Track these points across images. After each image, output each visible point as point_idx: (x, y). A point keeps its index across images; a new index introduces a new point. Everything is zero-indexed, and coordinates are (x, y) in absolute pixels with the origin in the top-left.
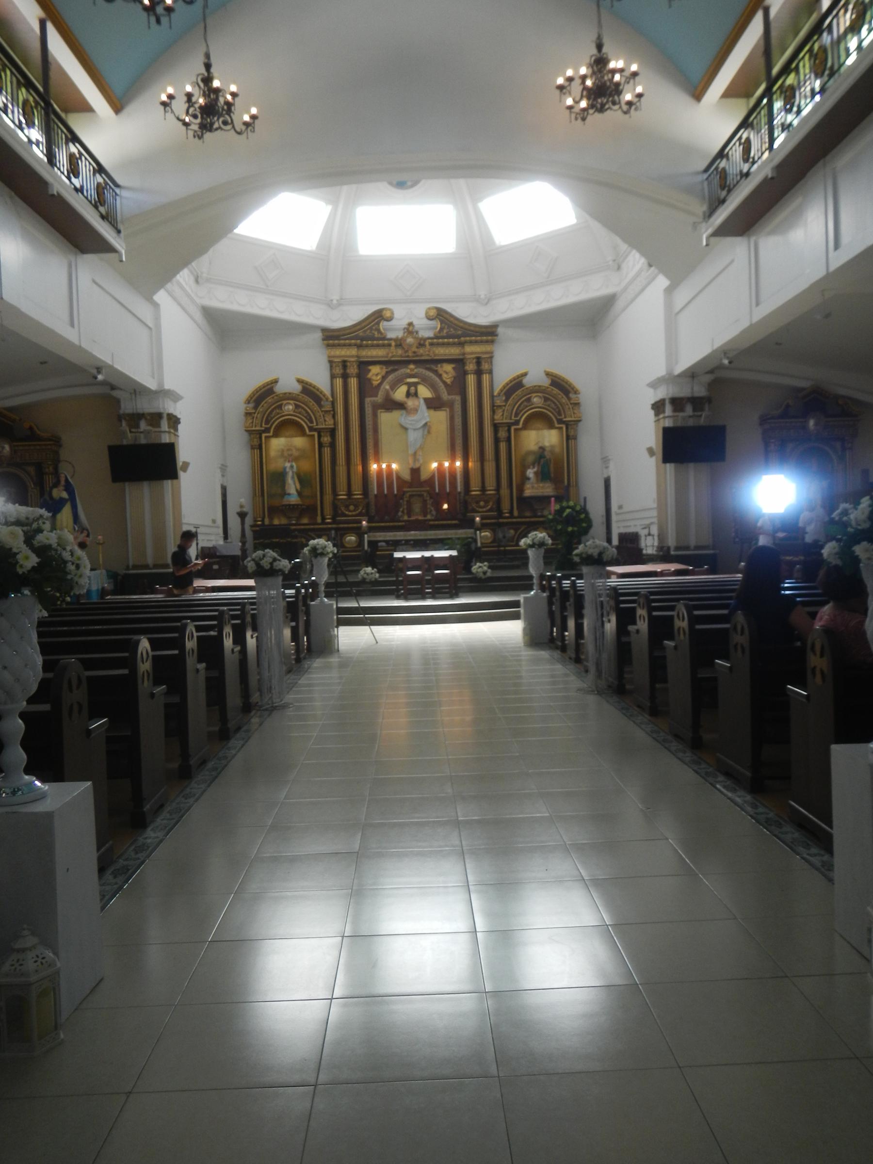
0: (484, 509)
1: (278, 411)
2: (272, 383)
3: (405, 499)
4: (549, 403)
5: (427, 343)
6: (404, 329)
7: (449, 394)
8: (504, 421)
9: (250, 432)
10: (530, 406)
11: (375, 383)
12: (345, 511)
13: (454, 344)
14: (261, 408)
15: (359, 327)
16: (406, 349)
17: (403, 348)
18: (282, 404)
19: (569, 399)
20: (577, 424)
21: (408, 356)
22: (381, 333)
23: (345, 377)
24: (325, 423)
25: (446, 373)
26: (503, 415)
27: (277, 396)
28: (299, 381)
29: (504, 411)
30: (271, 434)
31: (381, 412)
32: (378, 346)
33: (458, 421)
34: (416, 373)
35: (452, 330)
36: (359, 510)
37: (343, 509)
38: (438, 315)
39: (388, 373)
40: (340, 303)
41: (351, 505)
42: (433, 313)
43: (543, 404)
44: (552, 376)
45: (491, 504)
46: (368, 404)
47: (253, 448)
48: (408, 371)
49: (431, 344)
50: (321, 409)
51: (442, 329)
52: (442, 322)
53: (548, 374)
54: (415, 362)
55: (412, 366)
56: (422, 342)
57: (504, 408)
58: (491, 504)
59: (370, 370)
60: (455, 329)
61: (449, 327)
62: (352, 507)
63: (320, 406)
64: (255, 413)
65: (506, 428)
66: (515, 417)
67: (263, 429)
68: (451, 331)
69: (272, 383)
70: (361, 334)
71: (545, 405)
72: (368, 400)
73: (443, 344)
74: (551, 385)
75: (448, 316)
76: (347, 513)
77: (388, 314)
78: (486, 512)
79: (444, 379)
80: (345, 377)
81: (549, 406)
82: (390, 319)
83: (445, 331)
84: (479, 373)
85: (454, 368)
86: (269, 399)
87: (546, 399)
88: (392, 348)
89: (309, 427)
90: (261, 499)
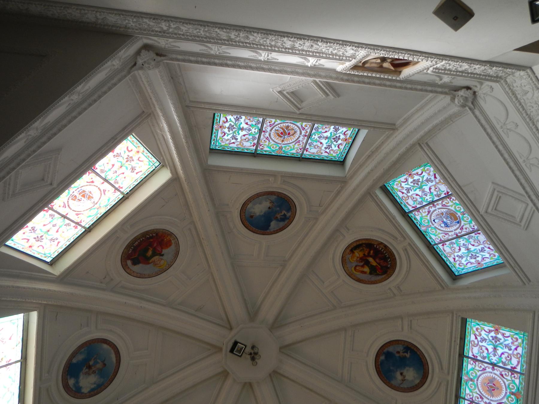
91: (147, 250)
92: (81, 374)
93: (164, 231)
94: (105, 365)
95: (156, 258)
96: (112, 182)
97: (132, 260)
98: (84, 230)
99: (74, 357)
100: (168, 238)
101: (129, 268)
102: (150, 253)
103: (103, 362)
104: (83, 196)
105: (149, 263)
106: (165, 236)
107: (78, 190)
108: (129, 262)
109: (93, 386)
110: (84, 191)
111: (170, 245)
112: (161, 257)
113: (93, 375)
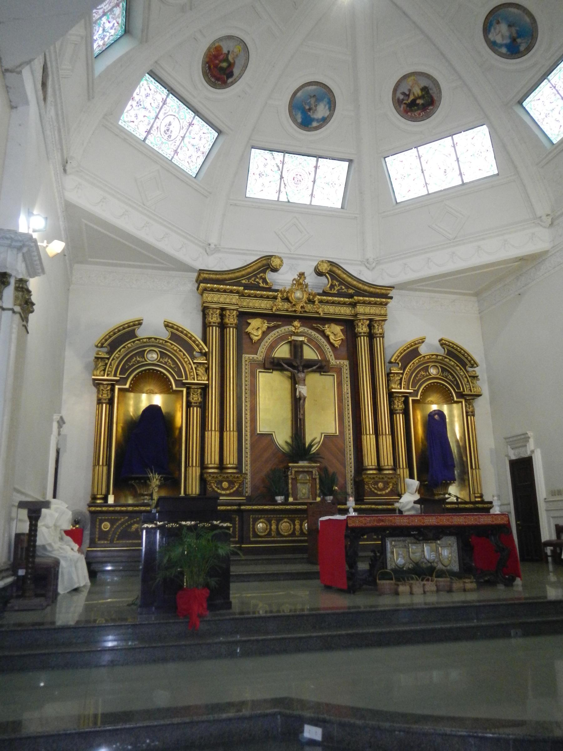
0: (384, 492)
1: (138, 359)
2: (134, 325)
3: (290, 476)
4: (446, 374)
5: (316, 299)
6: (294, 280)
7: (336, 358)
8: (402, 390)
9: (97, 384)
10: (427, 376)
11: (255, 338)
12: (216, 489)
13: (344, 304)
14: (117, 353)
15: (243, 273)
16: (294, 303)
17: (291, 303)
18: (145, 351)
19: (467, 372)
20: (473, 399)
21: (295, 311)
22: (267, 283)
23: (223, 326)
24: (197, 378)
25: (335, 335)
26: (400, 384)
27: (138, 340)
28: (167, 325)
29: (401, 379)
30: (127, 386)
31: (259, 372)
32: (261, 297)
33: (347, 388)
34: (301, 332)
35: (343, 287)
36: (235, 489)
37: (214, 487)
38: (329, 271)
39: (269, 329)
40: (217, 249)
41: (225, 481)
42: (324, 268)
43: (440, 376)
44: (449, 346)
45: (391, 484)
46: (246, 361)
47: (99, 402)
48: (293, 329)
49: (321, 302)
50: (193, 361)
51: (332, 286)
52: (333, 278)
53: (443, 343)
54: (300, 318)
55: (296, 323)
56: (311, 297)
57: (401, 376)
58: (391, 484)
59: (249, 324)
60: (347, 287)
61: (341, 284)
62: (225, 484)
63: (193, 357)
64: (108, 359)
65: (403, 398)
66: (412, 388)
67: (118, 378)
68: (344, 289)
69: (134, 325)
70: (244, 282)
71: (443, 376)
72: (246, 357)
73: (333, 303)
74: (447, 355)
75: (339, 272)
76: (219, 491)
77: (275, 262)
78: (386, 495)
79: (332, 341)
80: (223, 326)
81: (446, 377)
82: (275, 270)
83: (336, 288)
84: (371, 337)
85: (341, 330)
86: (129, 344)
87: (443, 370)
88: (277, 300)
89: (176, 381)
90: (105, 468)
91: (222, 69)
92: (312, 116)
93: (205, 56)
94: (314, 96)
95: (230, 58)
96: (158, 110)
97: (228, 78)
98: (196, 117)
99: (297, 120)
100: (212, 51)
101: (235, 80)
102: (224, 65)
103: (311, 97)
104: (168, 130)
105: (234, 62)
106: (210, 55)
107: (163, 137)
108: (230, 80)
109: (327, 107)
110: (165, 131)
111: (220, 47)
112: (230, 53)
113: (318, 107)
